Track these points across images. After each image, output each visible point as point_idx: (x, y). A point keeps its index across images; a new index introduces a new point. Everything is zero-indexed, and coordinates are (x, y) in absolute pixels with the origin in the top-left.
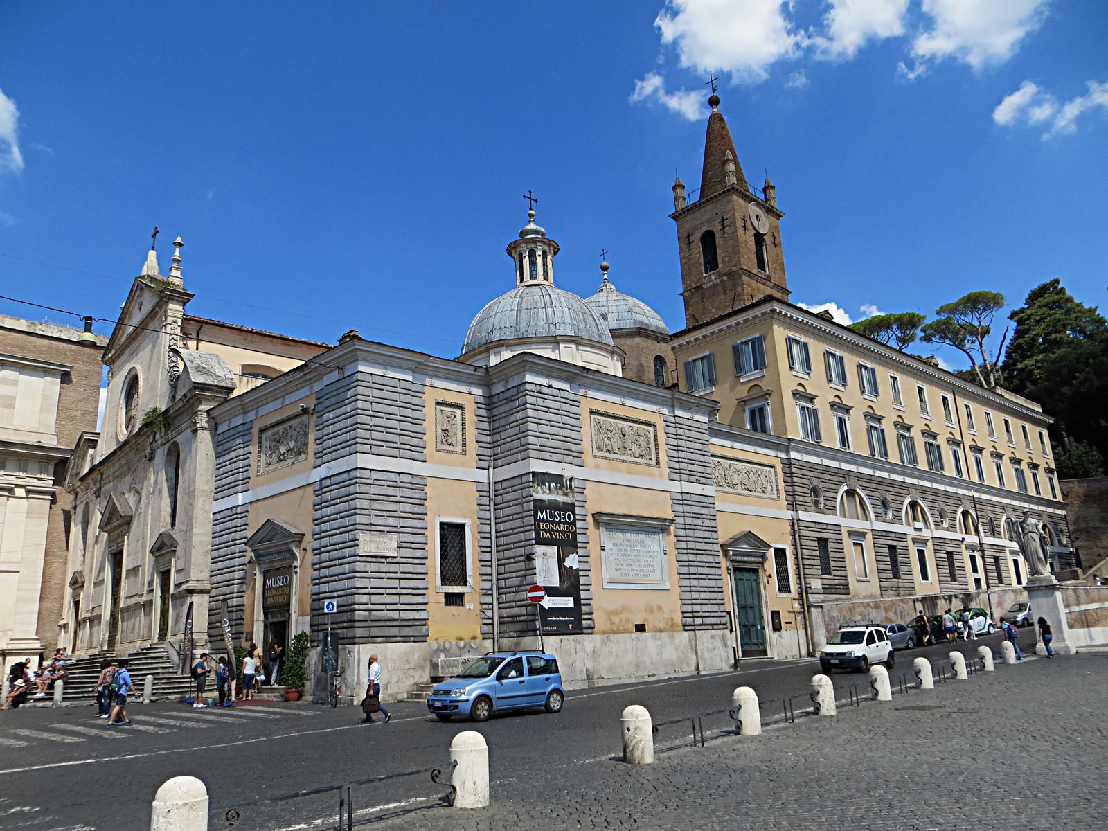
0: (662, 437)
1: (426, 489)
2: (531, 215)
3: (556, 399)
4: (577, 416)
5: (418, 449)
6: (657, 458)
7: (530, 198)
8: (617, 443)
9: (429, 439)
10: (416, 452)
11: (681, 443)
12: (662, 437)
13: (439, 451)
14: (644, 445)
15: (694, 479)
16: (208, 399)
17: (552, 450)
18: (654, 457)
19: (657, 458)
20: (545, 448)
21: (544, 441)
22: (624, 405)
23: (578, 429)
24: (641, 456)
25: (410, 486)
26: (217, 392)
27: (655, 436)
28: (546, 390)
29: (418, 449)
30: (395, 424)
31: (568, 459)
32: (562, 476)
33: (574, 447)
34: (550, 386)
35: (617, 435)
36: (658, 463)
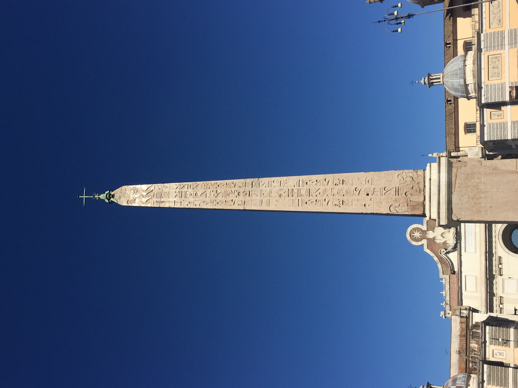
0: (492, 53)
1: (514, 121)
2: (418, 82)
3: (487, 93)
4: (491, 85)
5: (504, 124)
6: (499, 54)
7: (412, 83)
8: (496, 70)
9: (501, 121)
10: (505, 124)
11: (492, 46)
12: (492, 53)
13: (504, 117)
14: (495, 59)
15: (503, 39)
16: (486, 152)
17: (502, 94)
18: (498, 55)
19: (499, 54)
20: (502, 95)
21: (500, 97)
22: (484, 68)
23: (495, 85)
24: (499, 61)
25: (514, 125)
26: (483, 151)
27: (492, 55)
28: (486, 97)
29: (504, 124)
30: (499, 130)
31: (504, 89)
32: (510, 91)
33: (500, 87)
34: (484, 95)
35: (494, 70)
36: (500, 54)
